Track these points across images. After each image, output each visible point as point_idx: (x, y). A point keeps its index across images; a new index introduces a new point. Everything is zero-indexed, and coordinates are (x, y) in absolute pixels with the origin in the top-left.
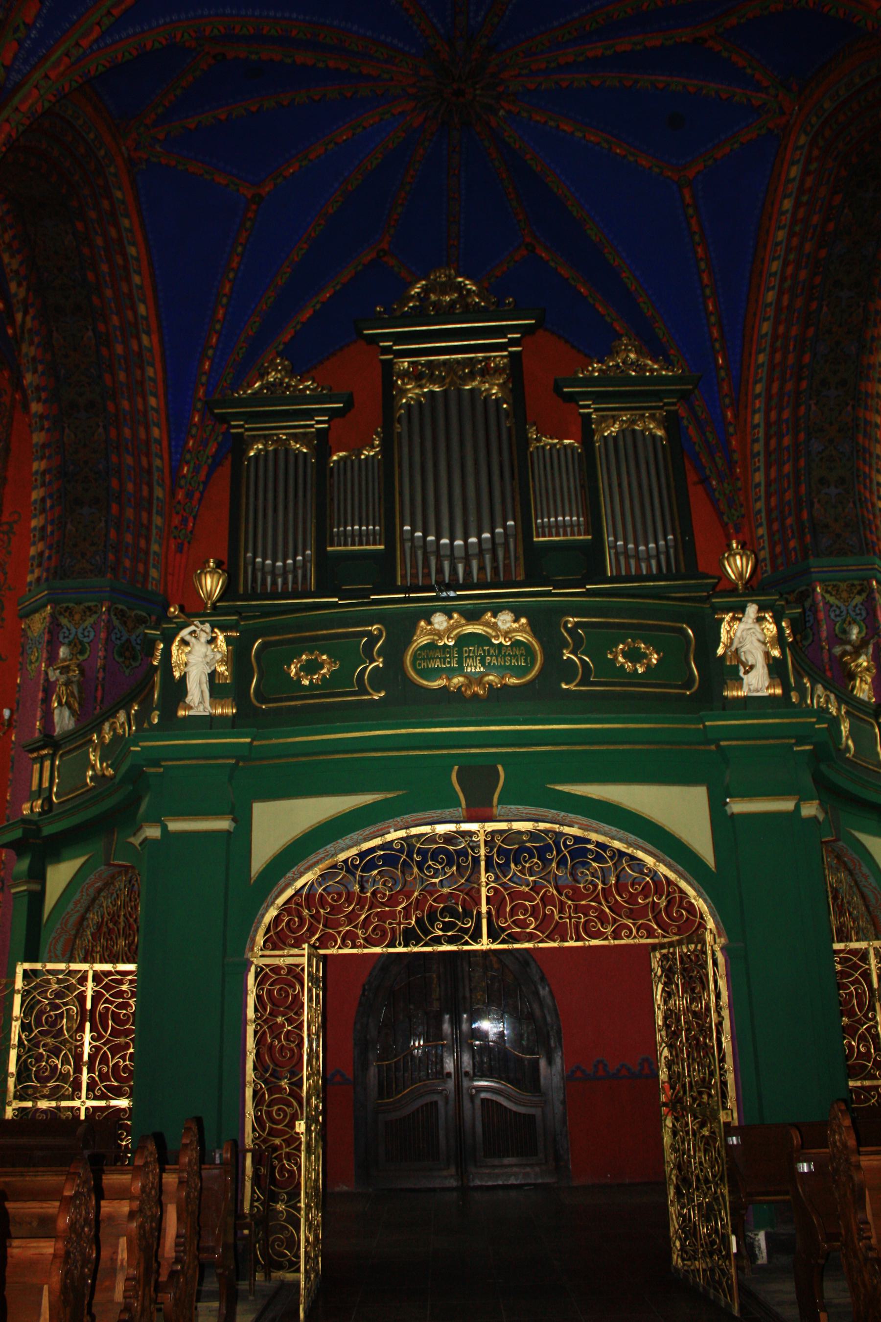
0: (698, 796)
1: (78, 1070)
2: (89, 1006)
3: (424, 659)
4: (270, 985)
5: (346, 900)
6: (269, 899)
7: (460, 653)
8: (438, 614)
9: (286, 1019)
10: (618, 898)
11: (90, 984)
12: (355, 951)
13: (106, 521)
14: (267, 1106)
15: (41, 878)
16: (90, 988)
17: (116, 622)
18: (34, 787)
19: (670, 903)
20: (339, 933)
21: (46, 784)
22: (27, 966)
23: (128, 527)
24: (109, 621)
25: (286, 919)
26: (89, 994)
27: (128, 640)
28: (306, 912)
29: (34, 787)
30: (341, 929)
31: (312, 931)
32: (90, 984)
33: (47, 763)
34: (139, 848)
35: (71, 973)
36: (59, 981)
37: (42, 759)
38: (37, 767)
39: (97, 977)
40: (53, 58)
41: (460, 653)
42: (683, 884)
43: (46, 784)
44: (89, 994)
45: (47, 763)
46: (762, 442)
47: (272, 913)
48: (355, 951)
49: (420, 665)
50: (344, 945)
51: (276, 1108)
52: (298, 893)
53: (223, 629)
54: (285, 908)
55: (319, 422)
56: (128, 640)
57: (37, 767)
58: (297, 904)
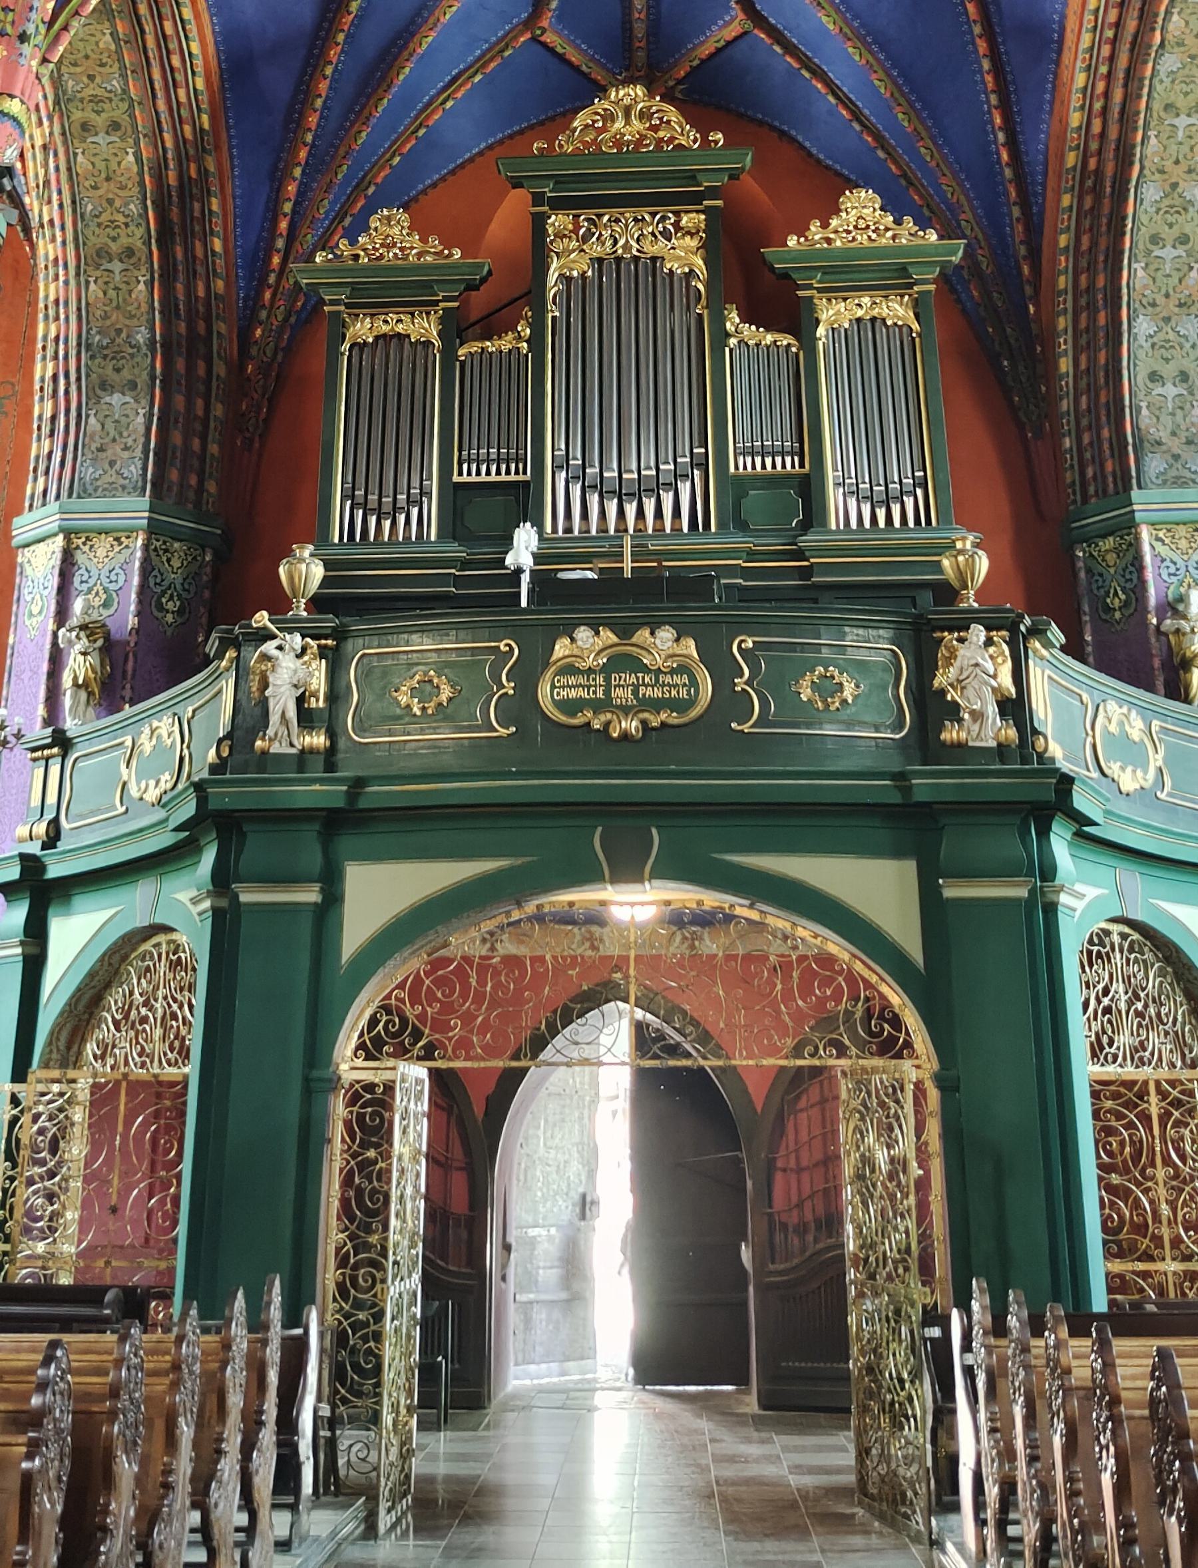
3: (563, 687)
4: (362, 1107)
5: (460, 995)
7: (608, 680)
8: (582, 628)
9: (380, 1154)
10: (800, 1003)
12: (468, 1064)
14: (352, 1269)
20: (450, 1039)
23: (176, 421)
25: (385, 1018)
30: (450, 1034)
34: (197, 918)
41: (608, 680)
42: (885, 989)
46: (1070, 315)
48: (468, 1064)
49: (558, 694)
51: (362, 1271)
58: (397, 999)
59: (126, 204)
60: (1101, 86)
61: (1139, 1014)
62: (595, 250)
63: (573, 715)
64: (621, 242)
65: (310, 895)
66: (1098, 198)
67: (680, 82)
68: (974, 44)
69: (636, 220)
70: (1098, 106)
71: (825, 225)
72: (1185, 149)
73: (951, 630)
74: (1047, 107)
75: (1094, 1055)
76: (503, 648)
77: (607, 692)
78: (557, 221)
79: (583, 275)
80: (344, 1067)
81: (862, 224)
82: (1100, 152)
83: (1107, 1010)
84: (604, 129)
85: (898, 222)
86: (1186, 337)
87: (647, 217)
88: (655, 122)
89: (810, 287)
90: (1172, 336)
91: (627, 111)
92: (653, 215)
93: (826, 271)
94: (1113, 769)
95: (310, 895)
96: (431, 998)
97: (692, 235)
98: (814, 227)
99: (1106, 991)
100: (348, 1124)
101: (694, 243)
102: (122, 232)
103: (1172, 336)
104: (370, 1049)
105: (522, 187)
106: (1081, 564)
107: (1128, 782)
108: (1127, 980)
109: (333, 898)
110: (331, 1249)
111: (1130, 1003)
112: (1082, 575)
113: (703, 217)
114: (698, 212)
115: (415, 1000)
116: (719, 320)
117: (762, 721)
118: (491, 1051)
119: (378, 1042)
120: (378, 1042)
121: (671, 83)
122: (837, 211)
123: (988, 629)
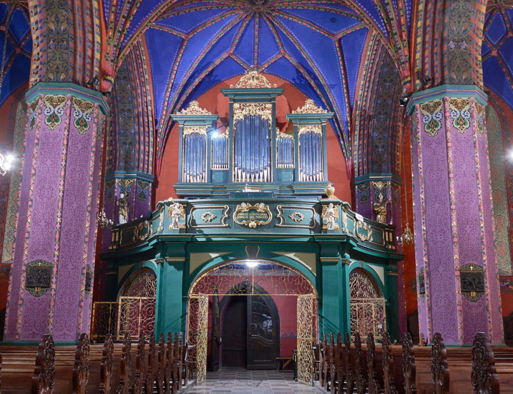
0: (313, 256)
1: (137, 327)
2: (140, 309)
6: (194, 280)
11: (141, 303)
13: (135, 151)
15: (117, 270)
16: (141, 304)
17: (139, 186)
18: (113, 240)
19: (304, 285)
21: (117, 240)
22: (122, 297)
24: (136, 185)
26: (140, 306)
27: (142, 192)
28: (204, 284)
29: (113, 240)
31: (206, 289)
32: (141, 303)
33: (117, 233)
35: (136, 300)
36: (132, 302)
37: (115, 232)
38: (113, 234)
39: (143, 301)
40: (134, 38)
43: (117, 240)
44: (140, 306)
45: (117, 233)
47: (195, 284)
50: (215, 293)
52: (203, 278)
53: (183, 204)
54: (199, 283)
55: (208, 124)
56: (142, 192)
57: (113, 234)
59: (128, 98)
60: (369, 75)
61: (362, 288)
62: (244, 112)
63: (241, 222)
64: (251, 111)
65: (182, 260)
66: (366, 102)
67: (266, 68)
68: (339, 62)
69: (255, 105)
70: (368, 79)
71: (301, 108)
72: (388, 91)
73: (326, 204)
74: (356, 79)
75: (352, 296)
76: (225, 207)
77: (249, 217)
78: (236, 105)
79: (242, 119)
80: (190, 295)
81: (310, 108)
82: (367, 91)
83: (355, 286)
84: (247, 82)
85: (319, 108)
86: (385, 137)
87: (258, 105)
88: (260, 80)
89: (297, 123)
90: (381, 137)
91: (253, 77)
92: (259, 104)
93: (301, 119)
94: (360, 235)
95: (182, 260)
96: (209, 281)
97: (269, 110)
98: (299, 108)
99: (355, 282)
100: (191, 307)
101: (270, 112)
102: (127, 105)
103: (381, 137)
104: (196, 291)
105: (227, 96)
106: (356, 190)
107: (363, 238)
108: (360, 281)
109: (187, 260)
110: (188, 332)
111: (360, 285)
112: (357, 192)
113: (271, 105)
114: (270, 104)
115: (206, 282)
116: (275, 131)
117: (282, 224)
118: (222, 292)
119: (198, 290)
120: (198, 290)
121: (264, 69)
122: (304, 105)
123: (334, 204)
